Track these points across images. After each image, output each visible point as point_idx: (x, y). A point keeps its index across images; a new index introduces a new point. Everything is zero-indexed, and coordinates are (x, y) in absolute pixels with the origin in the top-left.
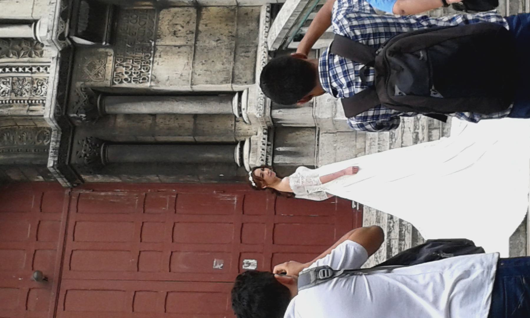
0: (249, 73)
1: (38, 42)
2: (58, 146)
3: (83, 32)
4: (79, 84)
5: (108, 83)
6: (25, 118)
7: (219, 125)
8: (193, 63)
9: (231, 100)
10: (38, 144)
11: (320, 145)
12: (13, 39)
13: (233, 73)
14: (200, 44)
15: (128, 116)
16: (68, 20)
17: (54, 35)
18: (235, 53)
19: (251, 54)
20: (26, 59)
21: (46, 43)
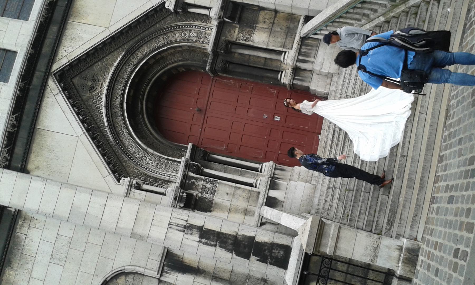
0: (290, 45)
1: (210, 17)
3: (229, 17)
4: (223, 38)
5: (234, 40)
6: (201, 48)
7: (274, 64)
8: (269, 37)
9: (281, 55)
10: (204, 59)
11: (313, 79)
12: (201, 14)
13: (284, 44)
14: (273, 29)
15: (240, 54)
16: (223, 11)
17: (217, 16)
18: (287, 35)
19: (293, 37)
20: (204, 24)
21: (213, 18)
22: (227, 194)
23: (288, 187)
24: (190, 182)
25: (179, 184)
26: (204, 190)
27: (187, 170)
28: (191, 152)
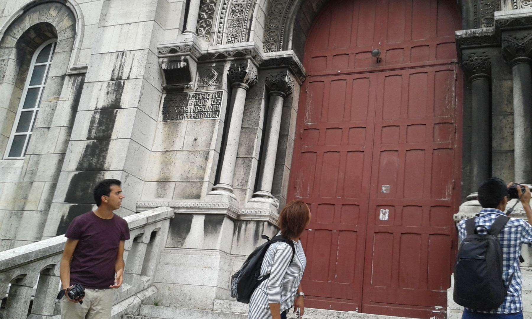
2: (477, 35)
22: (196, 140)
23: (209, 253)
24: (213, 70)
25: (206, 52)
26: (200, 98)
27: (233, 58)
28: (276, 59)
